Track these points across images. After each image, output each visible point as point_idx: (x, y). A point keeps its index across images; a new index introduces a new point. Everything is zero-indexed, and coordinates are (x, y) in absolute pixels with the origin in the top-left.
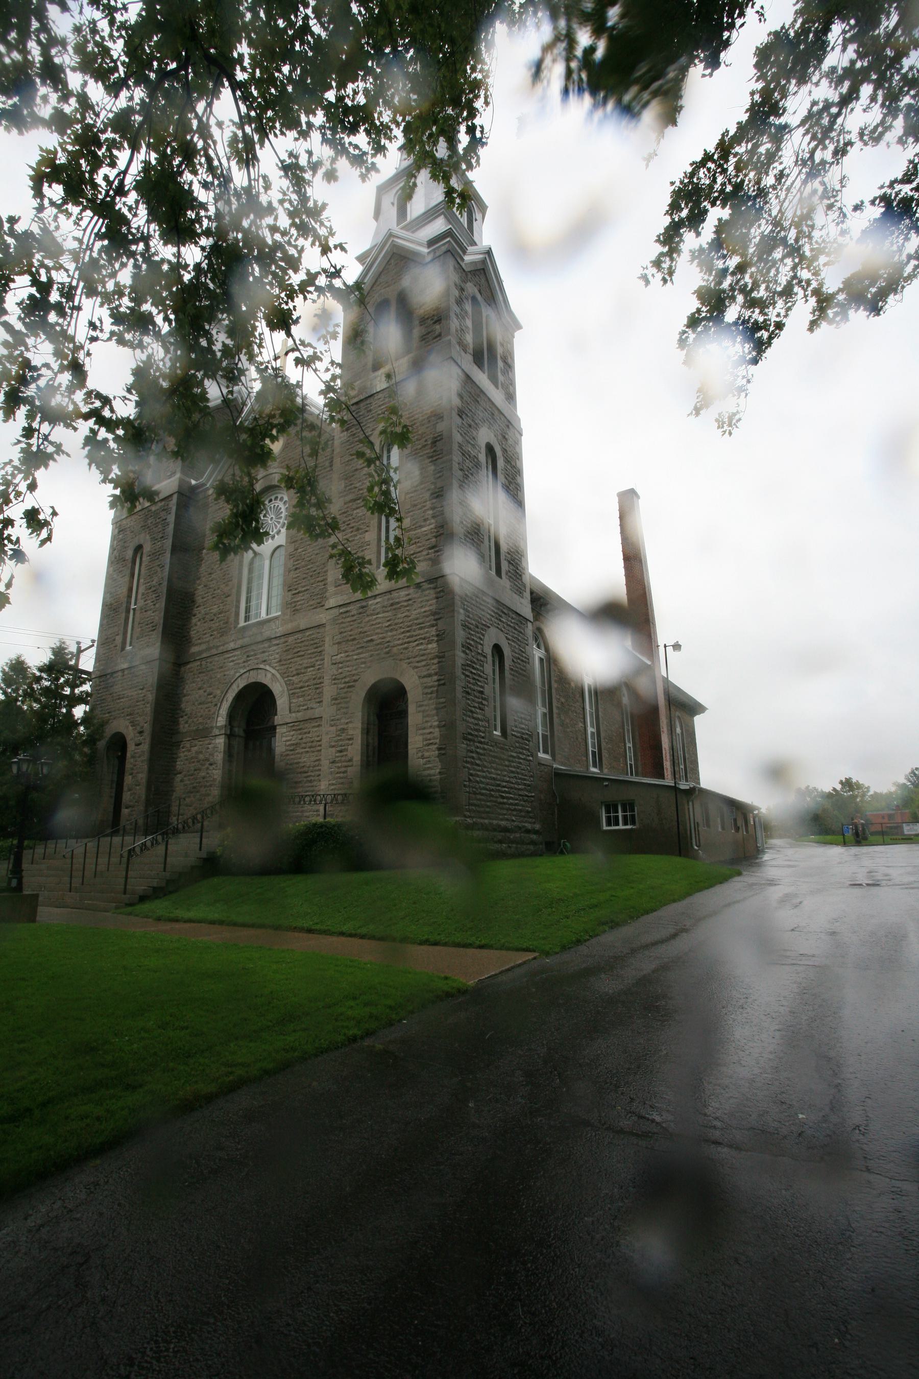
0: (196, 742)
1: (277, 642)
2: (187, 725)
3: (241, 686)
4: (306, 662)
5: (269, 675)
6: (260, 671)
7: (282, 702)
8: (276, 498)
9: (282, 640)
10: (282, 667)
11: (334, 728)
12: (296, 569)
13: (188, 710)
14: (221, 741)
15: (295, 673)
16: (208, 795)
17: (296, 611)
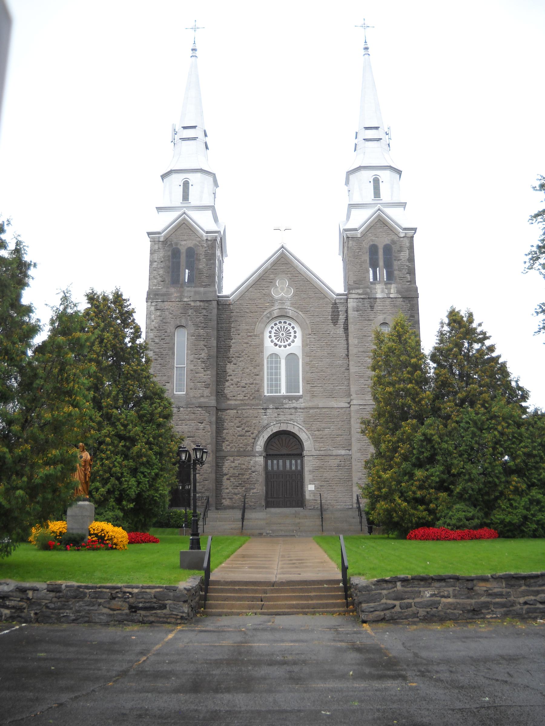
0: (239, 458)
1: (302, 411)
2: (229, 447)
3: (274, 431)
4: (324, 425)
5: (296, 428)
6: (288, 424)
7: (308, 444)
8: (285, 323)
9: (306, 410)
10: (307, 425)
11: (360, 463)
12: (312, 373)
13: (229, 438)
14: (260, 460)
15: (316, 429)
16: (253, 489)
17: (313, 396)
